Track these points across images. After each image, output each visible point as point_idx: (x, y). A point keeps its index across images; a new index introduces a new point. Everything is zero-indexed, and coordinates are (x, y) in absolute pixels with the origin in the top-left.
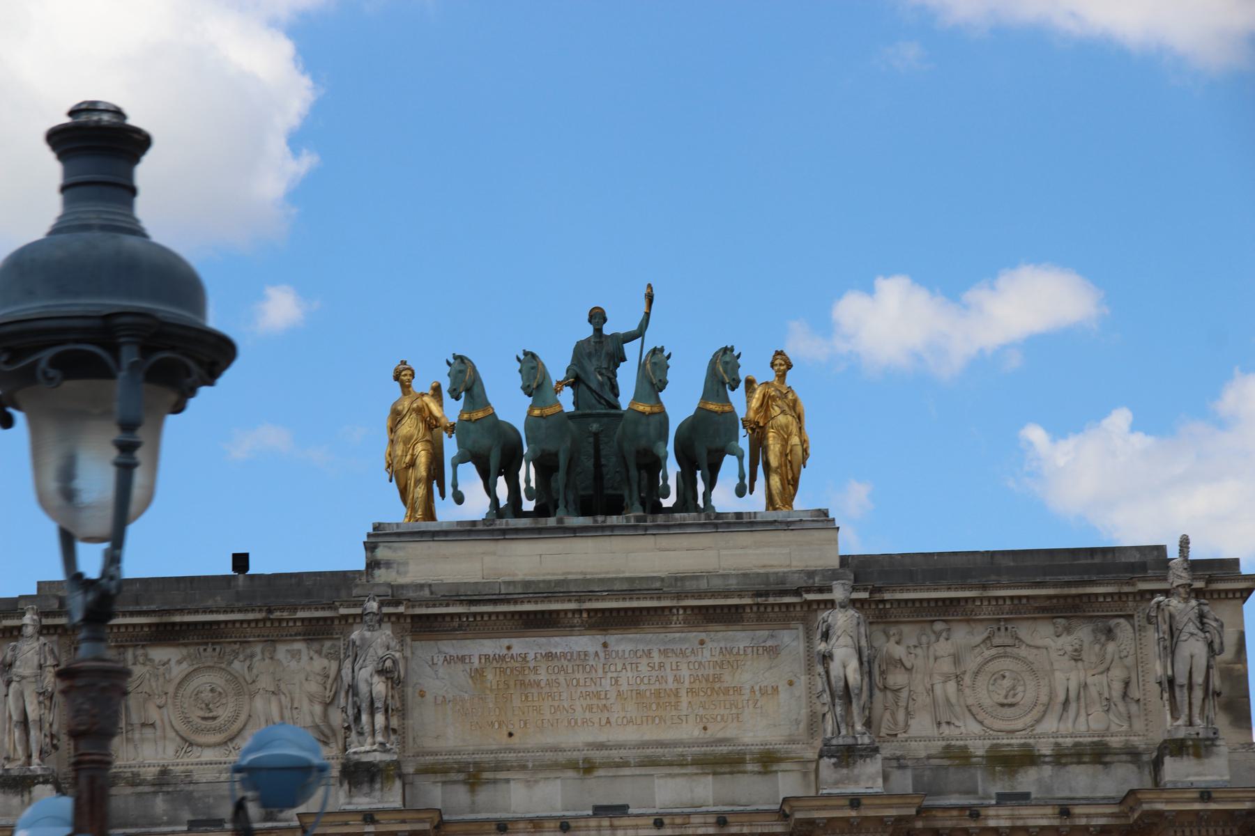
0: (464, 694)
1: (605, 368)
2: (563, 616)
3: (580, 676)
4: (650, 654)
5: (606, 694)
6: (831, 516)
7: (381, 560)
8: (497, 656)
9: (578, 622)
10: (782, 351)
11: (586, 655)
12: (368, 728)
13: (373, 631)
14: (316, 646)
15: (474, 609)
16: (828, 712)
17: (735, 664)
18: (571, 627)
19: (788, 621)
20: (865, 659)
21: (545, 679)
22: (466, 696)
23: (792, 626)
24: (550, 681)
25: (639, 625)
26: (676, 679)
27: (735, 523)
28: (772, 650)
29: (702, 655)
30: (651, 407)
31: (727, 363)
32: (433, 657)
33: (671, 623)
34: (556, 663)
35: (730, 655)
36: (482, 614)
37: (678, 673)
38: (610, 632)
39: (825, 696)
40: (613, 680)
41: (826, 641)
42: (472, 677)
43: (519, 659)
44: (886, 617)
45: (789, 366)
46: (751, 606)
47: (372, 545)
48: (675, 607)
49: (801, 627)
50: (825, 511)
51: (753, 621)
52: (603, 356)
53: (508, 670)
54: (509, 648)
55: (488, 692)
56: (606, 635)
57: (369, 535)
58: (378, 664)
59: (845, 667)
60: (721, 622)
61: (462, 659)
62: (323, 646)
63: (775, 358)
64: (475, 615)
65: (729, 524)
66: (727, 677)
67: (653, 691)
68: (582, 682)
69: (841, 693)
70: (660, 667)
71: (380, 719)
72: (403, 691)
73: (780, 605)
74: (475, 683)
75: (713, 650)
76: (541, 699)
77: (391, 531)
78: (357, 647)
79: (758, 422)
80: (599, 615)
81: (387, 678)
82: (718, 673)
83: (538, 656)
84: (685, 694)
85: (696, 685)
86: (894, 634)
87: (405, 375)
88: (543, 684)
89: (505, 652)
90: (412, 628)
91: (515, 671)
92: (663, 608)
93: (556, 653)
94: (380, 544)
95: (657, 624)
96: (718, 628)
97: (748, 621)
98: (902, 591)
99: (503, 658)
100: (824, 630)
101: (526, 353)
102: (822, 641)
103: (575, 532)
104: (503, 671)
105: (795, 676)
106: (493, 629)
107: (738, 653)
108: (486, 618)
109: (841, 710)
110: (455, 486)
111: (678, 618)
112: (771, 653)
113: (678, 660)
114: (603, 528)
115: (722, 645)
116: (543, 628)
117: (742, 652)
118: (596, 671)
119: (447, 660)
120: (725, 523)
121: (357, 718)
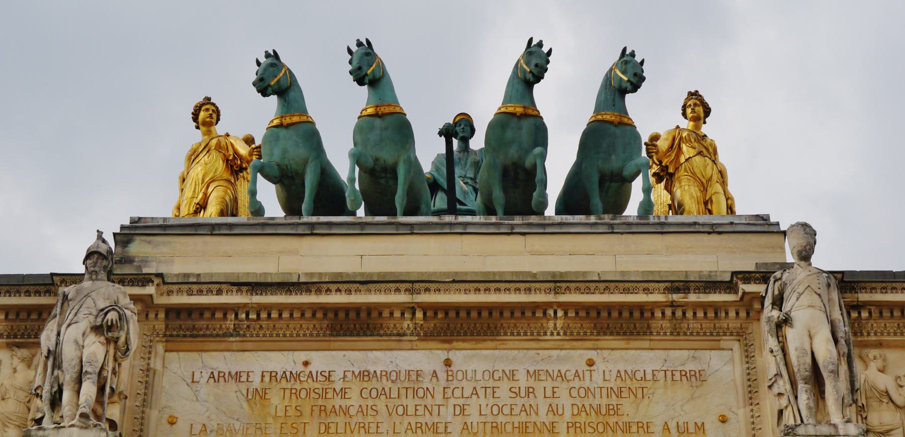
0: (235, 422)
1: (471, 178)
2: (388, 315)
3: (410, 403)
4: (513, 375)
5: (446, 427)
6: (773, 220)
7: (134, 257)
8: (288, 374)
9: (408, 328)
10: (697, 91)
11: (418, 375)
12: (69, 411)
13: (96, 279)
14: (24, 353)
15: (257, 299)
16: (786, 407)
17: (640, 391)
18: (399, 335)
19: (718, 335)
20: (840, 335)
21: (357, 405)
22: (237, 425)
23: (723, 344)
24: (364, 408)
25: (498, 334)
26: (551, 410)
27: (637, 224)
28: (695, 375)
29: (591, 380)
30: (524, 107)
31: (626, 62)
32: (193, 373)
33: (545, 334)
34: (374, 383)
35: (631, 379)
36: (268, 308)
37: (555, 401)
38: (455, 344)
39: (781, 382)
40: (458, 409)
41: (781, 310)
42: (248, 401)
43: (320, 378)
44: (862, 335)
45: (707, 111)
46: (661, 306)
47: (125, 239)
48: (550, 305)
49: (736, 346)
50: (765, 217)
51: (665, 334)
52: (468, 165)
53: (303, 393)
54: (306, 364)
55: (270, 420)
56: (450, 350)
57: (123, 227)
58: (97, 317)
59: (811, 337)
60: (618, 334)
61: (237, 377)
62: (34, 356)
63: (687, 99)
64: (259, 308)
65: (630, 224)
66: (627, 407)
67: (516, 425)
68: (411, 410)
69: (807, 373)
70: (528, 393)
71: (89, 389)
72: (143, 412)
73: (705, 306)
74: (252, 408)
75: (607, 373)
76: (348, 431)
77: (157, 224)
78: (71, 300)
79: (667, 167)
80: (440, 315)
81: (108, 341)
82: (615, 403)
83: (349, 375)
84: (566, 431)
85: (583, 418)
86: (875, 358)
87: (207, 110)
88: (353, 411)
89: (301, 368)
90: (167, 327)
91: (313, 395)
92: (535, 306)
93: (375, 372)
94: (138, 238)
95: (525, 334)
96: (614, 344)
97: (658, 334)
98: (884, 290)
99: (296, 377)
100: (776, 292)
101: (359, 44)
102: (773, 308)
103: (411, 230)
104: (296, 393)
105: (730, 410)
106: (285, 335)
107: (644, 378)
108: (274, 315)
109: (808, 399)
110: (253, 193)
111: (555, 325)
112: (693, 379)
113: (555, 384)
114: (450, 224)
115: (622, 368)
116: (358, 335)
117: (649, 377)
118: (433, 397)
119: (214, 377)
120: (624, 224)
121: (55, 402)
